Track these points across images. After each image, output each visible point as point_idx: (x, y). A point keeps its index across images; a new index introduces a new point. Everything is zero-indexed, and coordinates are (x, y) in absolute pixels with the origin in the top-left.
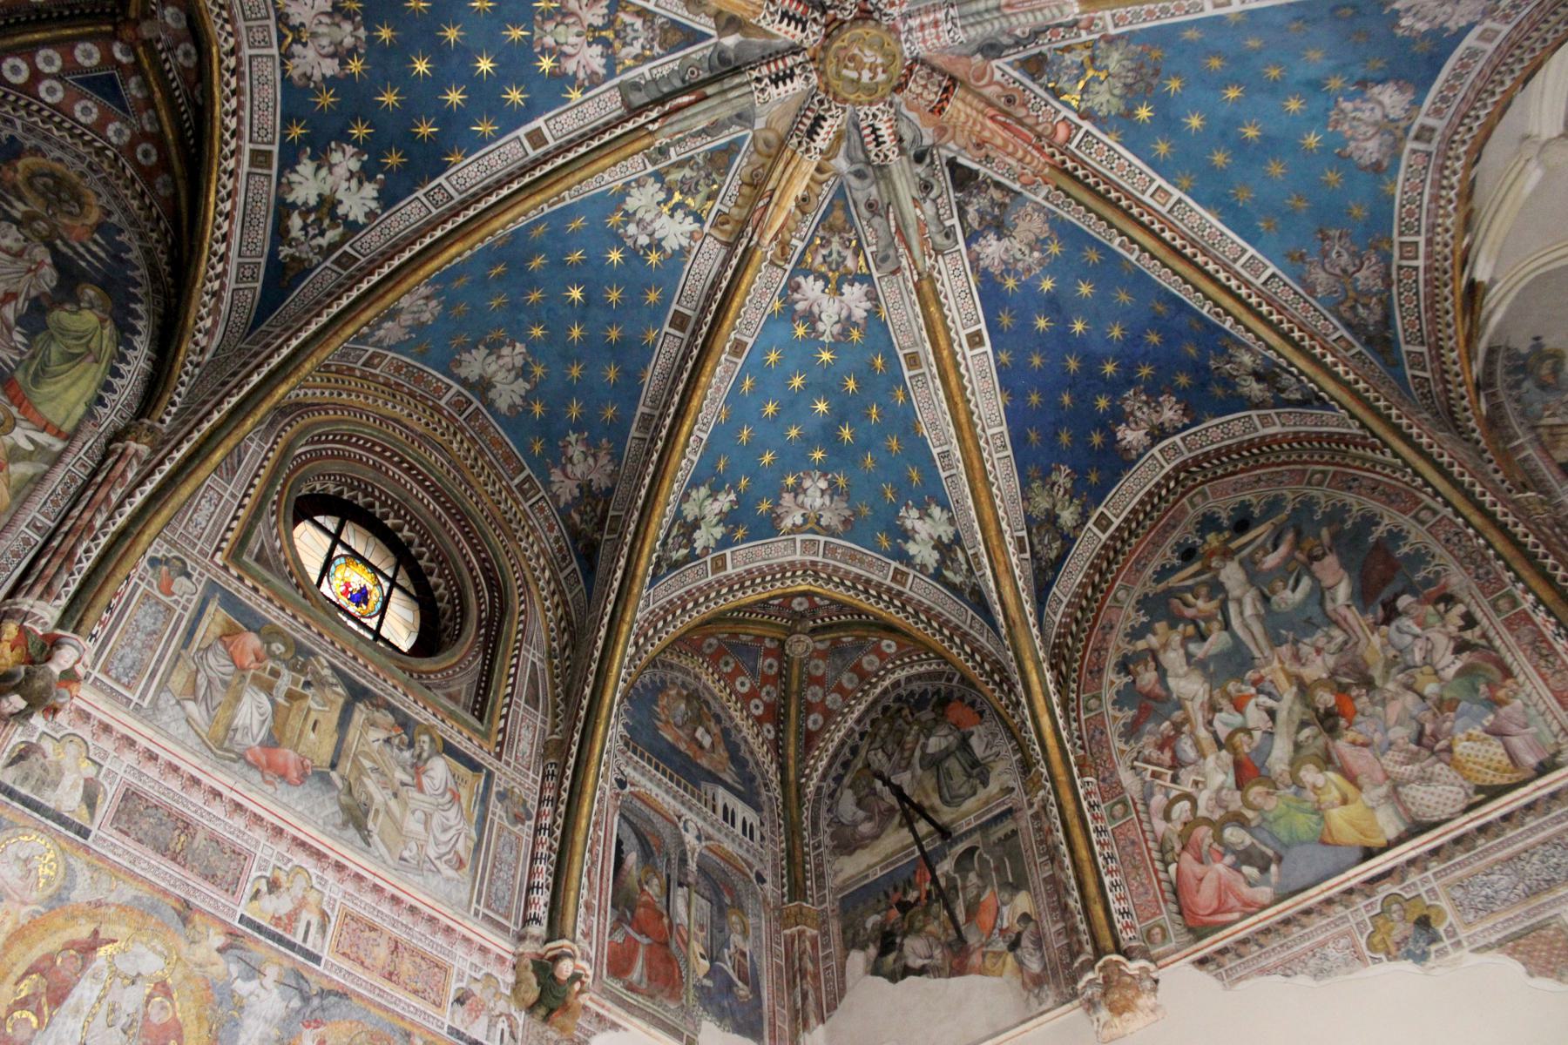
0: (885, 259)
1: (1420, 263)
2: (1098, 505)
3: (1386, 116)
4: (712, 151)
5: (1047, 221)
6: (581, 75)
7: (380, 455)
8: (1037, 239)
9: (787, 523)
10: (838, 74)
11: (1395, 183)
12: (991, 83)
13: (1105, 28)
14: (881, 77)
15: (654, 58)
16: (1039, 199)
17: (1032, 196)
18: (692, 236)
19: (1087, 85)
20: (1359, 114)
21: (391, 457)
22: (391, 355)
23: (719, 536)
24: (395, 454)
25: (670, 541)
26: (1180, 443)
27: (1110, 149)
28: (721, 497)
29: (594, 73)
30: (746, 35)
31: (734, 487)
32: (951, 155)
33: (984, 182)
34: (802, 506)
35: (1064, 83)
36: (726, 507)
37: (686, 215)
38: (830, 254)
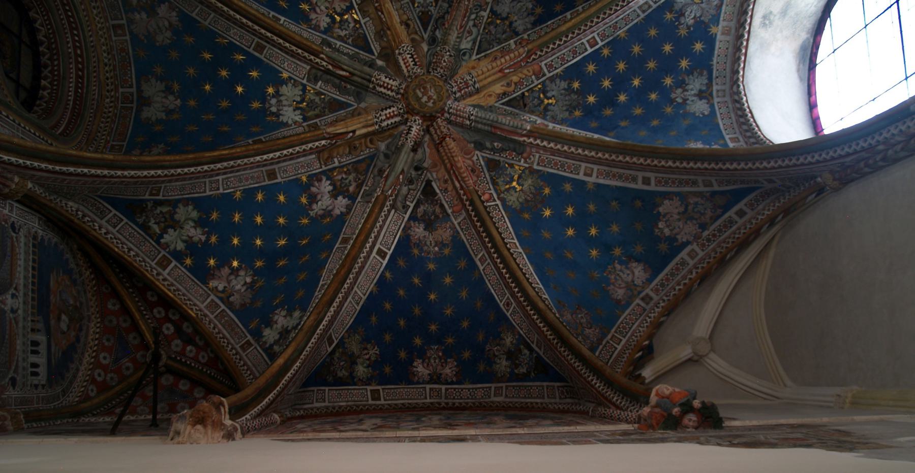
0: (368, 195)
1: (619, 347)
2: (380, 384)
3: (633, 281)
4: (335, 99)
5: (453, 236)
6: (314, 22)
7: (76, 55)
8: (442, 242)
9: (213, 284)
10: (414, 90)
11: (623, 312)
12: (470, 159)
13: (533, 163)
14: (430, 104)
15: (346, 43)
16: (456, 223)
17: (453, 219)
18: (295, 123)
19: (510, 188)
20: (621, 274)
21: (79, 63)
22: (128, 38)
23: (178, 248)
24: (82, 63)
25: (159, 209)
26: (443, 391)
27: (503, 216)
28: (199, 231)
29: (319, 26)
30: (387, 65)
31: (209, 234)
32: (431, 179)
33: (437, 201)
34: (229, 282)
35: (500, 181)
36: (196, 239)
37: (301, 114)
38: (346, 179)
